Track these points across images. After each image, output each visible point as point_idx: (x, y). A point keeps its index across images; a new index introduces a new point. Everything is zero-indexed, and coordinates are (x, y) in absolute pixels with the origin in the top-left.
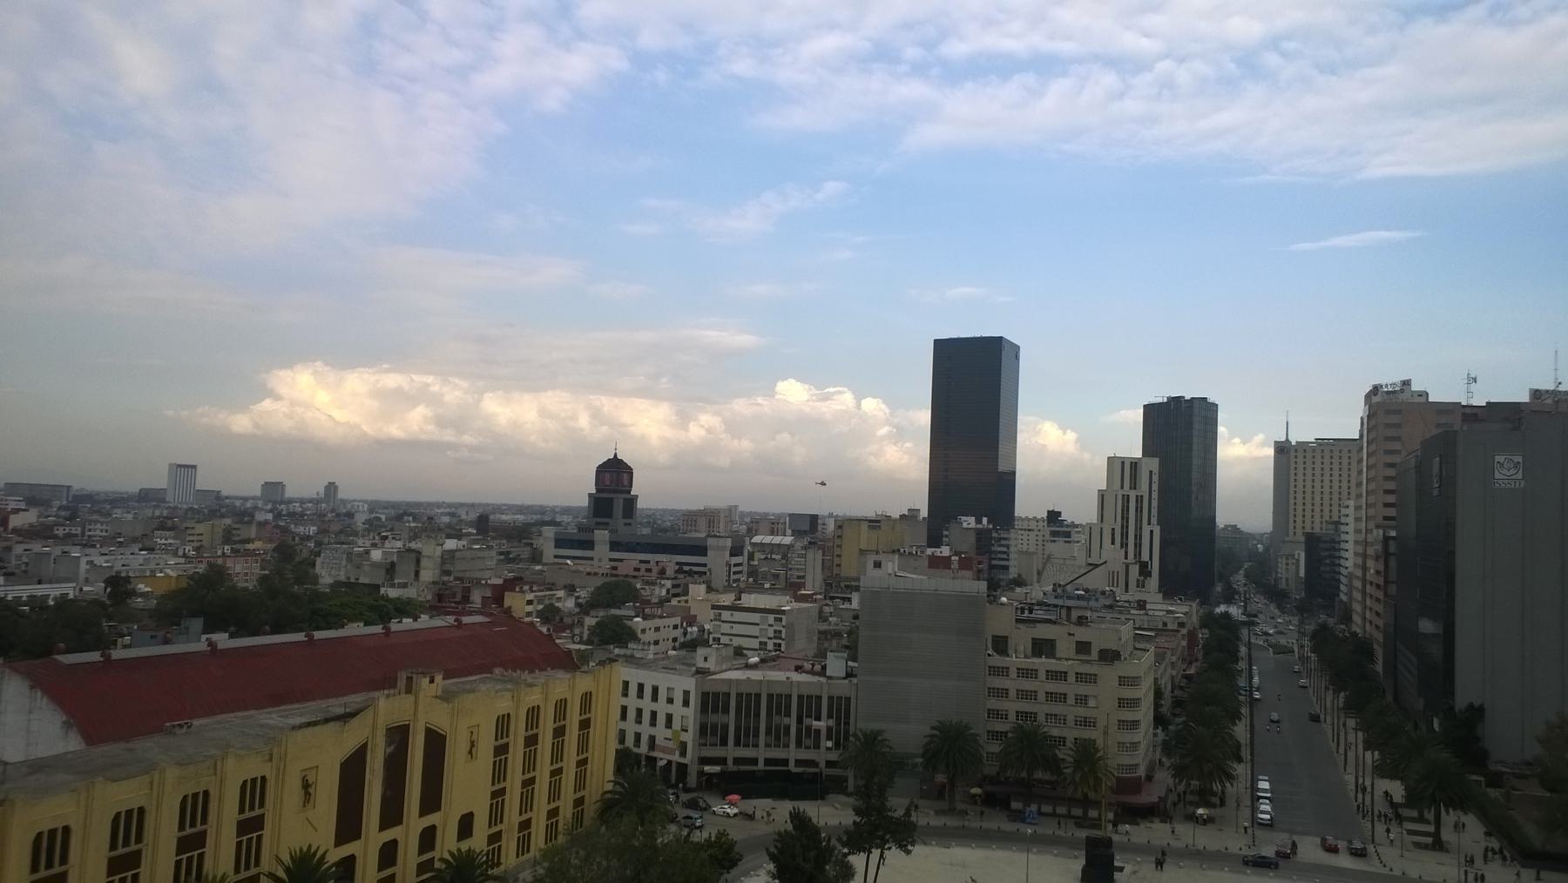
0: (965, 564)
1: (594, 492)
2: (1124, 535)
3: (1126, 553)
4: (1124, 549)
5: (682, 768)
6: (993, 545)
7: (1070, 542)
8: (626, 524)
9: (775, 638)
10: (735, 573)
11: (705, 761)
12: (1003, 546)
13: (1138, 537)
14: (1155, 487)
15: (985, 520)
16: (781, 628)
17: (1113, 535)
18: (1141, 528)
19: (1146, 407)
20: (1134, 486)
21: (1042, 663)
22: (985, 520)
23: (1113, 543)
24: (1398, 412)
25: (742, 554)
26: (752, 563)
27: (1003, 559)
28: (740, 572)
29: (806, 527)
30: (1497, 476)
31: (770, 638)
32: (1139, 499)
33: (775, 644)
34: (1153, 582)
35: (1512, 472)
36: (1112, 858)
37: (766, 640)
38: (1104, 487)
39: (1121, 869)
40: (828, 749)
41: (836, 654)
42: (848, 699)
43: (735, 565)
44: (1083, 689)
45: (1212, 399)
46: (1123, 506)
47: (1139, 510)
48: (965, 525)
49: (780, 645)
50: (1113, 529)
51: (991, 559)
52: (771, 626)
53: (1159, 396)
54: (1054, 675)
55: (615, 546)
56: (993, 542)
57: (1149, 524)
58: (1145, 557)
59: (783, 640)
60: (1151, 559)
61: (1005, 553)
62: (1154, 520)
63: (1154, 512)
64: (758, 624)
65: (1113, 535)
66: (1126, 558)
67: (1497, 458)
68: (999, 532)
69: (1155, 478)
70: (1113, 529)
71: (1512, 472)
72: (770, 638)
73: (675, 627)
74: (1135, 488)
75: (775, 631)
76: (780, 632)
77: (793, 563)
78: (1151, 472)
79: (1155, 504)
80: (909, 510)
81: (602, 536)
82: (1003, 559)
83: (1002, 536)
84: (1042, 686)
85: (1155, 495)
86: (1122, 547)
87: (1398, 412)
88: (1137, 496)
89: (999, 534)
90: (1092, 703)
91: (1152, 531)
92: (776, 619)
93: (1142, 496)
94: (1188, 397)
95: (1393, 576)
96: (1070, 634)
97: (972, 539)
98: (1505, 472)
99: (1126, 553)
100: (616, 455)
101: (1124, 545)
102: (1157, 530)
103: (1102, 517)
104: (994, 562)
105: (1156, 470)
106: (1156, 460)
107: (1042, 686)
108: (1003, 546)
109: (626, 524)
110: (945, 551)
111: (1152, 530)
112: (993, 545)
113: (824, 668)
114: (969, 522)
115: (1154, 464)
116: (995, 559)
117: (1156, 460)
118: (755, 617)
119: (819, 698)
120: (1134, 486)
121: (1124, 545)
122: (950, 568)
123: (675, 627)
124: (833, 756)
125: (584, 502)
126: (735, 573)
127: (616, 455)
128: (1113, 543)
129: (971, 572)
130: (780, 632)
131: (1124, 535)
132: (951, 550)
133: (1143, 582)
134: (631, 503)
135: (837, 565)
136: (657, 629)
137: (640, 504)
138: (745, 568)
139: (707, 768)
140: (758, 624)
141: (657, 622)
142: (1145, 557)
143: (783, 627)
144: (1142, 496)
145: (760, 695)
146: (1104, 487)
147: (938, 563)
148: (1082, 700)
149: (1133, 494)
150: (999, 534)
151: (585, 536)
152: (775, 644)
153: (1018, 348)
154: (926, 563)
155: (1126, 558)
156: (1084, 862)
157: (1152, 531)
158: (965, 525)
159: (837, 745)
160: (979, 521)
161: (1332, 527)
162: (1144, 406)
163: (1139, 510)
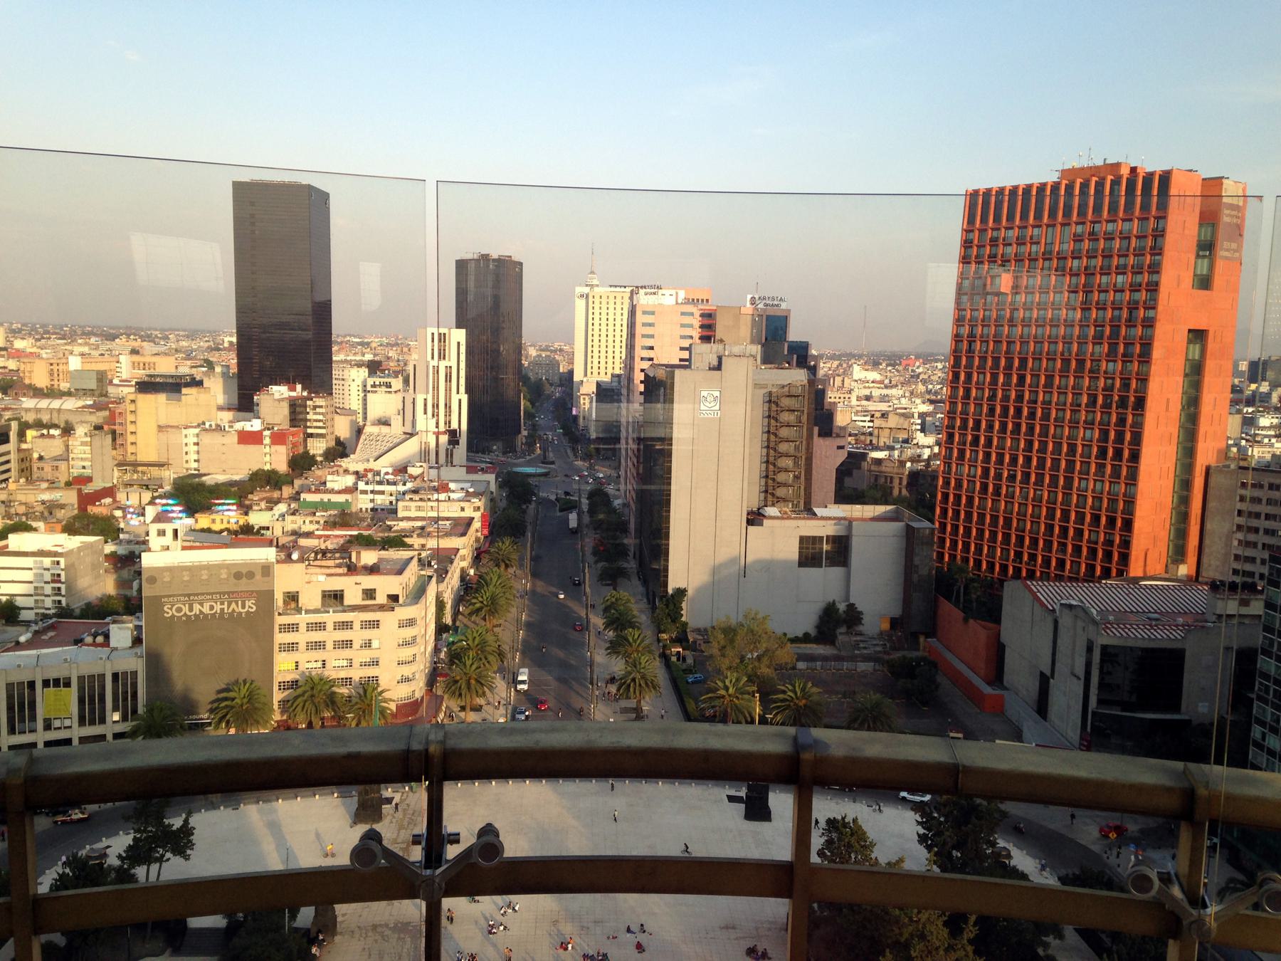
0: (278, 438)
2: (436, 406)
3: (437, 423)
4: (435, 419)
6: (308, 413)
7: (390, 392)
9: (53, 581)
12: (319, 414)
13: (448, 407)
14: (463, 357)
16: (59, 572)
17: (425, 405)
18: (450, 399)
19: (458, 262)
20: (442, 356)
21: (331, 617)
22: (299, 387)
23: (425, 413)
24: (653, 313)
26: (24, 446)
27: (320, 428)
29: (92, 384)
30: (703, 407)
31: (46, 583)
33: (53, 589)
35: (713, 404)
37: (43, 585)
40: (115, 722)
41: (119, 625)
44: (368, 634)
45: (516, 258)
49: (59, 589)
51: (307, 427)
52: (48, 569)
56: (308, 410)
57: (458, 393)
58: (454, 425)
59: (63, 583)
61: (320, 421)
62: (462, 389)
63: (463, 381)
64: (31, 569)
65: (425, 405)
66: (437, 427)
68: (314, 399)
71: (713, 404)
72: (46, 583)
75: (53, 575)
76: (59, 575)
77: (75, 451)
78: (459, 343)
79: (463, 373)
82: (320, 428)
83: (318, 404)
84: (330, 636)
85: (463, 365)
86: (433, 416)
87: (653, 313)
89: (314, 402)
90: (375, 644)
91: (460, 400)
93: (450, 367)
94: (495, 256)
95: (641, 460)
96: (356, 584)
97: (285, 410)
98: (707, 404)
99: (437, 423)
102: (465, 398)
104: (309, 431)
106: (464, 331)
107: (330, 636)
108: (319, 414)
110: (256, 425)
111: (461, 399)
112: (308, 413)
113: (107, 636)
115: (459, 336)
116: (310, 427)
117: (464, 331)
118: (28, 562)
119: (102, 676)
122: (261, 443)
124: (120, 728)
128: (425, 413)
129: (284, 447)
130: (59, 575)
131: (436, 406)
132: (263, 423)
133: (452, 451)
135: (132, 444)
140: (31, 569)
142: (454, 425)
143: (62, 570)
144: (450, 367)
145: (34, 682)
147: (249, 438)
148: (368, 645)
150: (314, 402)
152: (53, 589)
153: (328, 195)
154: (235, 439)
155: (437, 427)
157: (460, 400)
159: (124, 718)
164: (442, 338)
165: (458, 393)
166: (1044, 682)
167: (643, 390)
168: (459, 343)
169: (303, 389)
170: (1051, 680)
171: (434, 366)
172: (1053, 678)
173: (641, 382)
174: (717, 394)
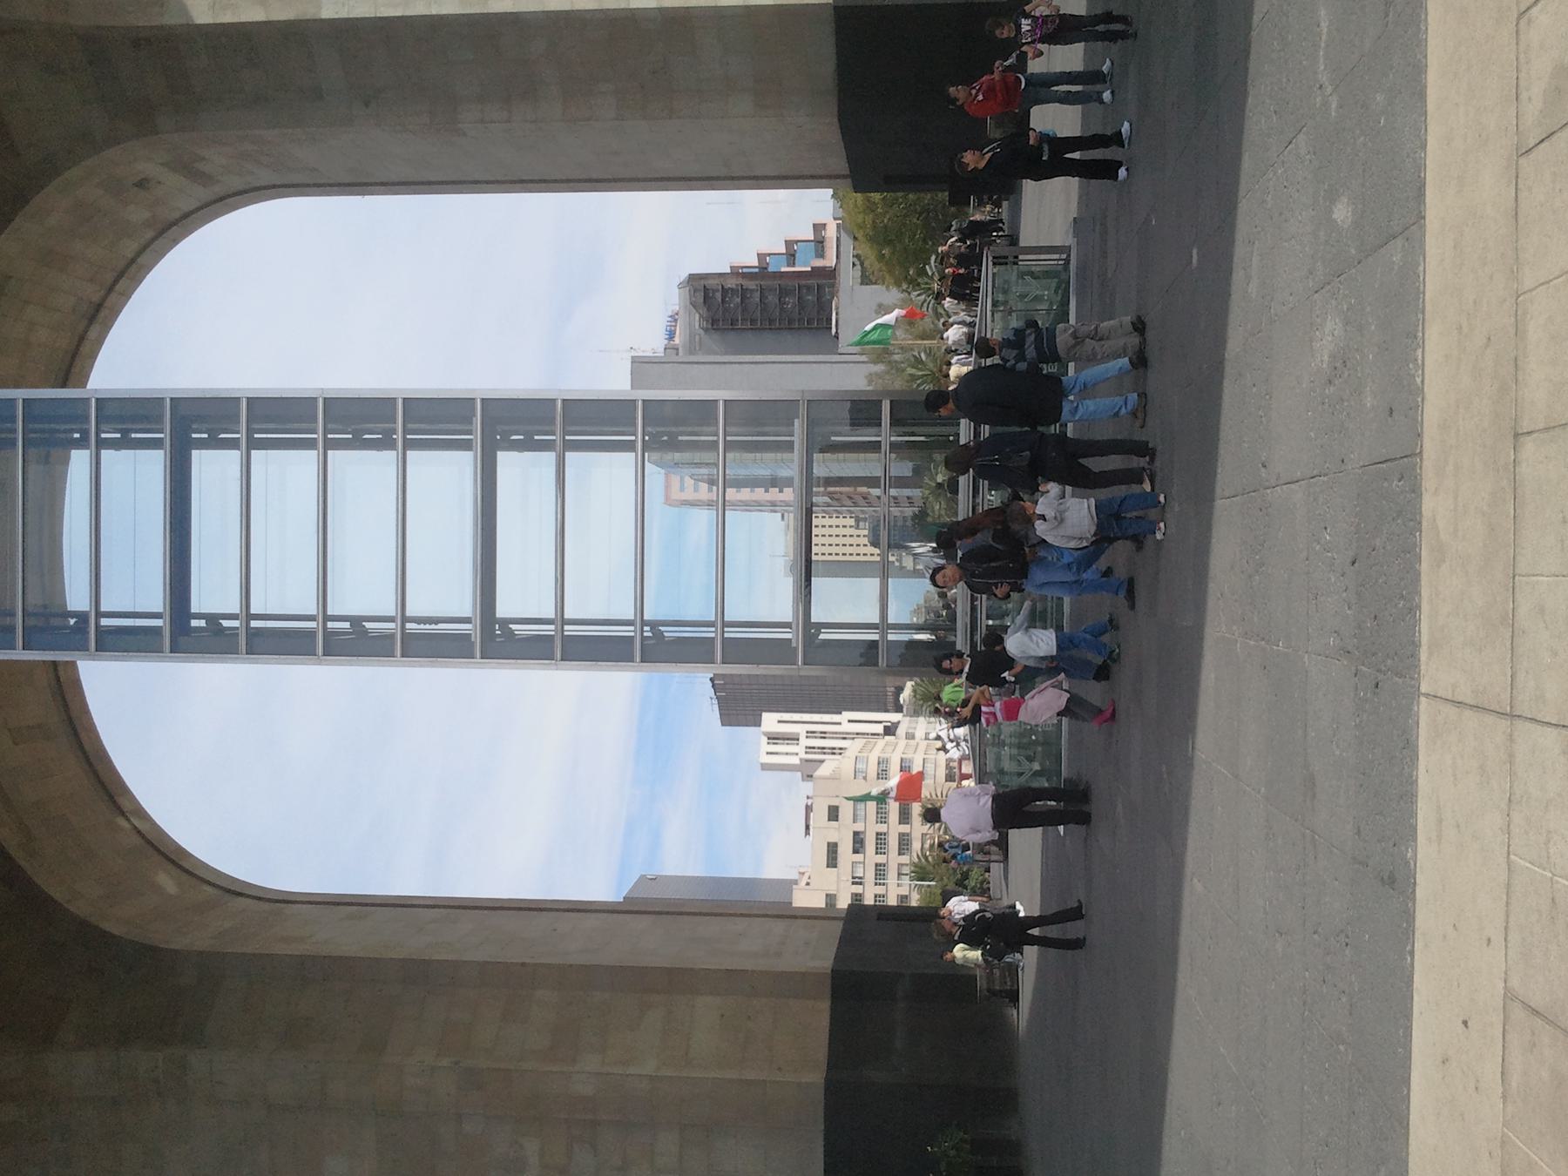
19: (723, 725)
20: (794, 739)
46: (819, 753)
47: (824, 735)
53: (712, 712)
57: (840, 724)
60: (881, 722)
74: (798, 740)
78: (779, 722)
88: (807, 737)
93: (807, 732)
102: (848, 715)
106: (765, 715)
115: (771, 721)
117: (765, 715)
120: (794, 739)
142: (879, 729)
146: (799, 774)
149: (804, 742)
161: (861, 524)
162: (723, 725)
163: (824, 735)
164: (774, 738)
165: (840, 724)
167: (763, 489)
168: (779, 722)
171: (806, 753)
173: (767, 491)
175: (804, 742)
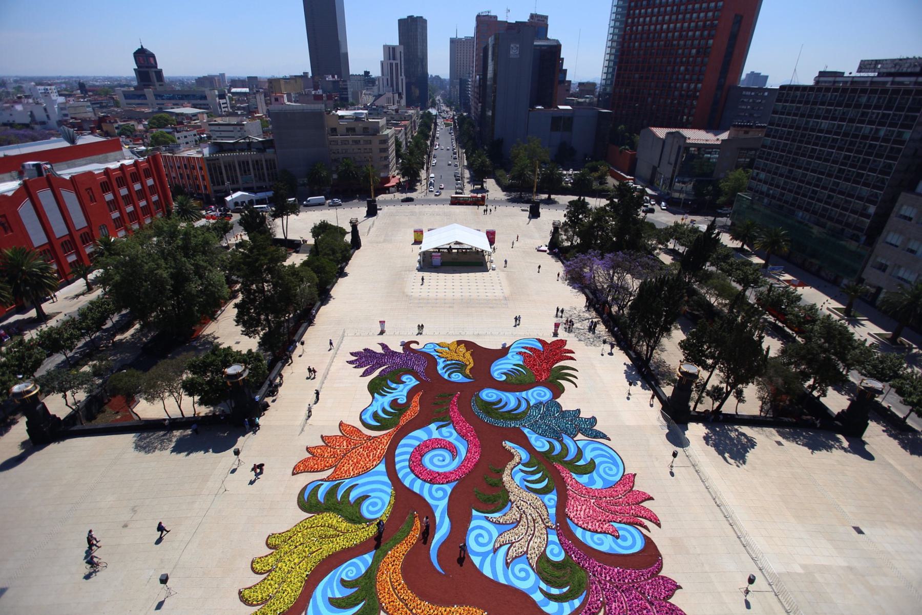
1: (136, 68)
5: (207, 196)
8: (160, 85)
10: (224, 108)
11: (216, 192)
14: (402, 59)
15: (336, 76)
22: (336, 76)
25: (225, 98)
28: (227, 107)
30: (511, 53)
32: (397, 64)
34: (403, 102)
36: (376, 206)
38: (383, 59)
39: (381, 209)
42: (274, 160)
43: (223, 104)
47: (397, 70)
48: (327, 79)
50: (387, 79)
54: (357, 142)
55: (158, 96)
58: (400, 91)
62: (403, 74)
63: (403, 70)
67: (512, 45)
69: (402, 55)
70: (387, 79)
73: (195, 135)
78: (400, 52)
80: (304, 73)
81: (149, 92)
85: (403, 63)
91: (402, 79)
92: (241, 129)
100: (142, 46)
101: (392, 85)
102: (404, 77)
103: (383, 74)
105: (402, 52)
109: (160, 85)
110: (320, 92)
114: (329, 78)
118: (231, 128)
121: (392, 85)
123: (195, 135)
125: (133, 74)
126: (224, 108)
127: (142, 46)
134: (159, 73)
136: (186, 137)
137: (166, 74)
138: (229, 105)
139: (218, 194)
141: (185, 133)
146: (383, 59)
151: (139, 93)
154: (313, 98)
156: (366, 209)
157: (402, 79)
158: (327, 79)
160: (333, 77)
163: (397, 70)
165: (401, 75)
166: (654, 169)
169: (338, 78)
170: (658, 169)
172: (659, 167)
174: (518, 46)
175: (394, 62)
